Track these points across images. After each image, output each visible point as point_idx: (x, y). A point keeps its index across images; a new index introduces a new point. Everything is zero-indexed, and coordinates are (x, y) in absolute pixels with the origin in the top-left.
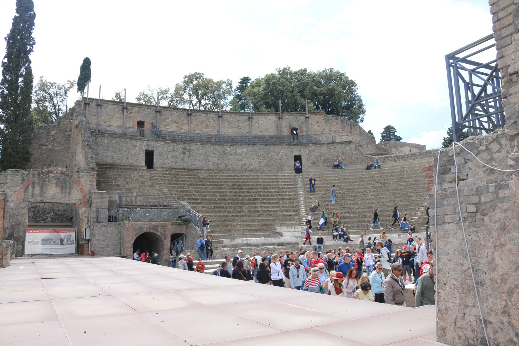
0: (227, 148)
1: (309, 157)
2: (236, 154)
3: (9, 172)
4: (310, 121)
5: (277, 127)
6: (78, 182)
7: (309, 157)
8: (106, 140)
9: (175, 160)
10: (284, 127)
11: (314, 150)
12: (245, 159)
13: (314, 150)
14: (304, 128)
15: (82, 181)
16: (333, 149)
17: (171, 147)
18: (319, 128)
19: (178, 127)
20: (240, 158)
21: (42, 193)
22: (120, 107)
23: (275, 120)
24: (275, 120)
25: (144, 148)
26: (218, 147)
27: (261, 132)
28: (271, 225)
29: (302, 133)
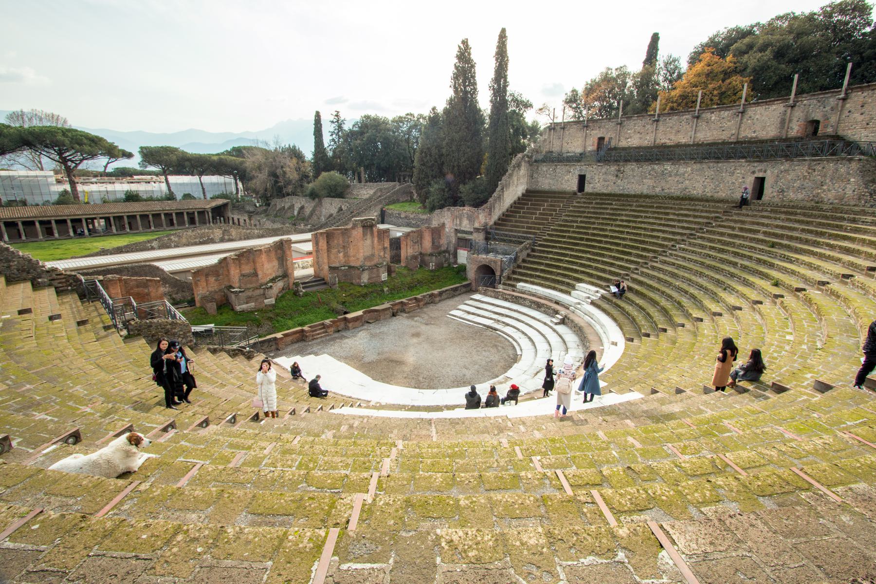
0: (668, 167)
1: (776, 182)
2: (676, 175)
3: (445, 209)
4: (848, 106)
5: (783, 122)
6: (478, 217)
7: (776, 182)
8: (545, 169)
9: (606, 183)
10: (795, 119)
11: (786, 171)
12: (687, 182)
13: (786, 171)
14: (833, 119)
15: (480, 216)
16: (819, 171)
17: (604, 170)
18: (863, 117)
19: (641, 138)
20: (681, 180)
21: (460, 224)
22: (581, 126)
23: (783, 109)
24: (783, 109)
25: (577, 173)
26: (656, 167)
27: (754, 132)
28: (580, 280)
29: (827, 129)
